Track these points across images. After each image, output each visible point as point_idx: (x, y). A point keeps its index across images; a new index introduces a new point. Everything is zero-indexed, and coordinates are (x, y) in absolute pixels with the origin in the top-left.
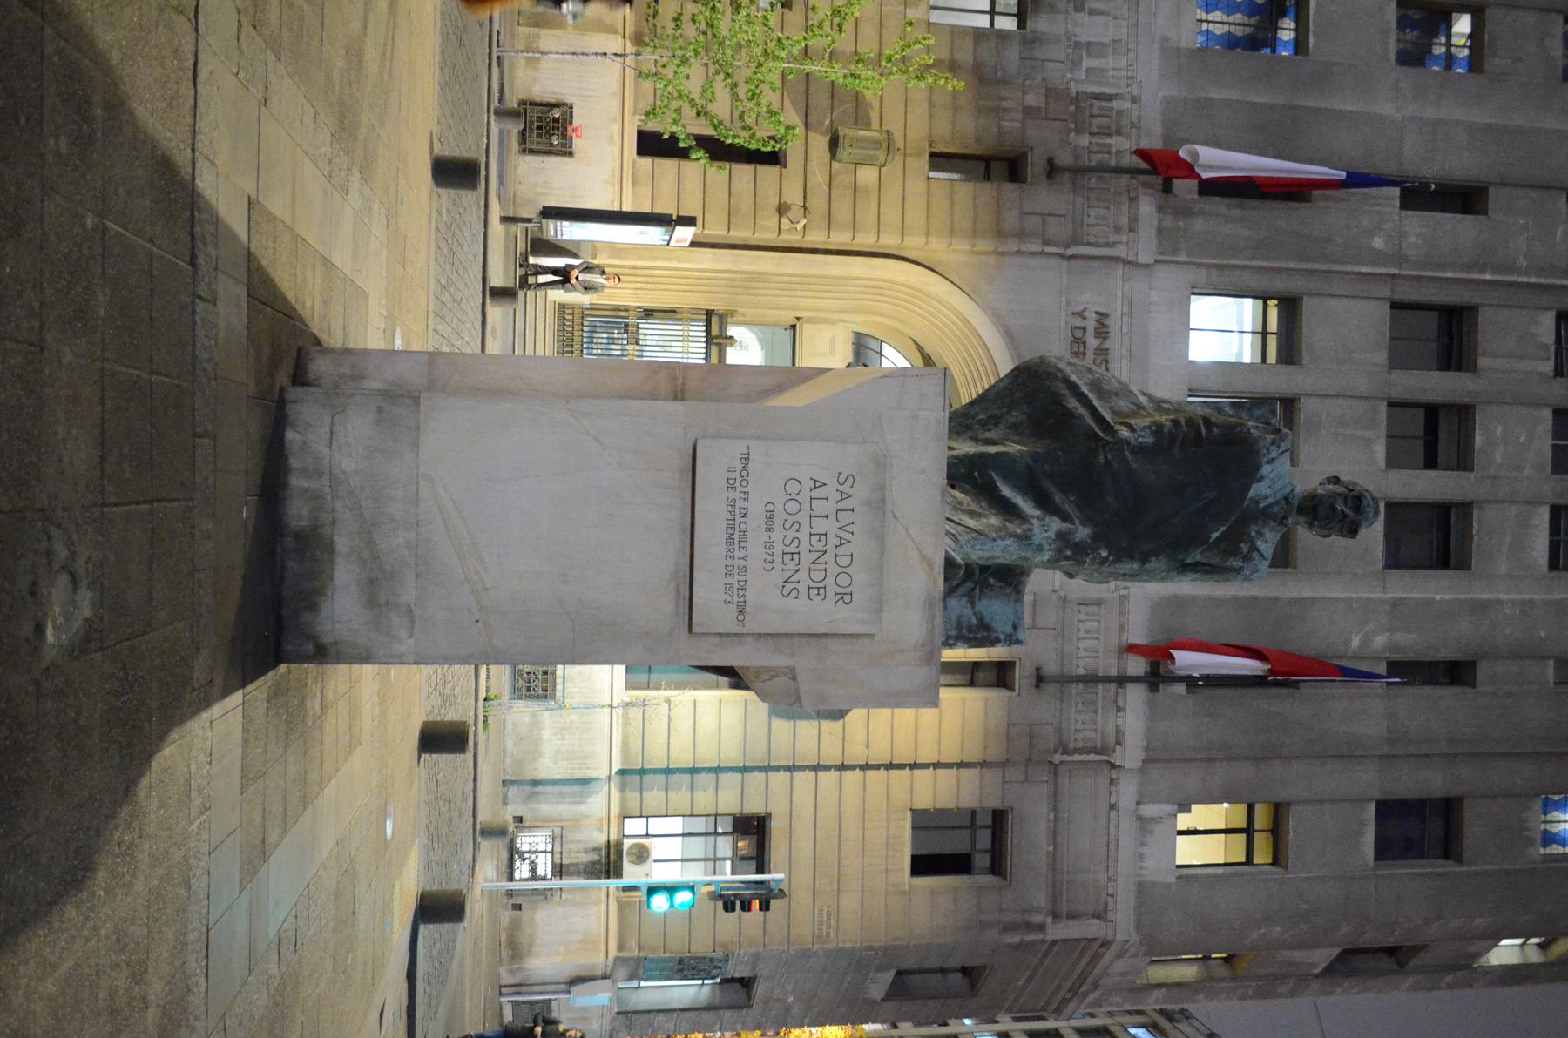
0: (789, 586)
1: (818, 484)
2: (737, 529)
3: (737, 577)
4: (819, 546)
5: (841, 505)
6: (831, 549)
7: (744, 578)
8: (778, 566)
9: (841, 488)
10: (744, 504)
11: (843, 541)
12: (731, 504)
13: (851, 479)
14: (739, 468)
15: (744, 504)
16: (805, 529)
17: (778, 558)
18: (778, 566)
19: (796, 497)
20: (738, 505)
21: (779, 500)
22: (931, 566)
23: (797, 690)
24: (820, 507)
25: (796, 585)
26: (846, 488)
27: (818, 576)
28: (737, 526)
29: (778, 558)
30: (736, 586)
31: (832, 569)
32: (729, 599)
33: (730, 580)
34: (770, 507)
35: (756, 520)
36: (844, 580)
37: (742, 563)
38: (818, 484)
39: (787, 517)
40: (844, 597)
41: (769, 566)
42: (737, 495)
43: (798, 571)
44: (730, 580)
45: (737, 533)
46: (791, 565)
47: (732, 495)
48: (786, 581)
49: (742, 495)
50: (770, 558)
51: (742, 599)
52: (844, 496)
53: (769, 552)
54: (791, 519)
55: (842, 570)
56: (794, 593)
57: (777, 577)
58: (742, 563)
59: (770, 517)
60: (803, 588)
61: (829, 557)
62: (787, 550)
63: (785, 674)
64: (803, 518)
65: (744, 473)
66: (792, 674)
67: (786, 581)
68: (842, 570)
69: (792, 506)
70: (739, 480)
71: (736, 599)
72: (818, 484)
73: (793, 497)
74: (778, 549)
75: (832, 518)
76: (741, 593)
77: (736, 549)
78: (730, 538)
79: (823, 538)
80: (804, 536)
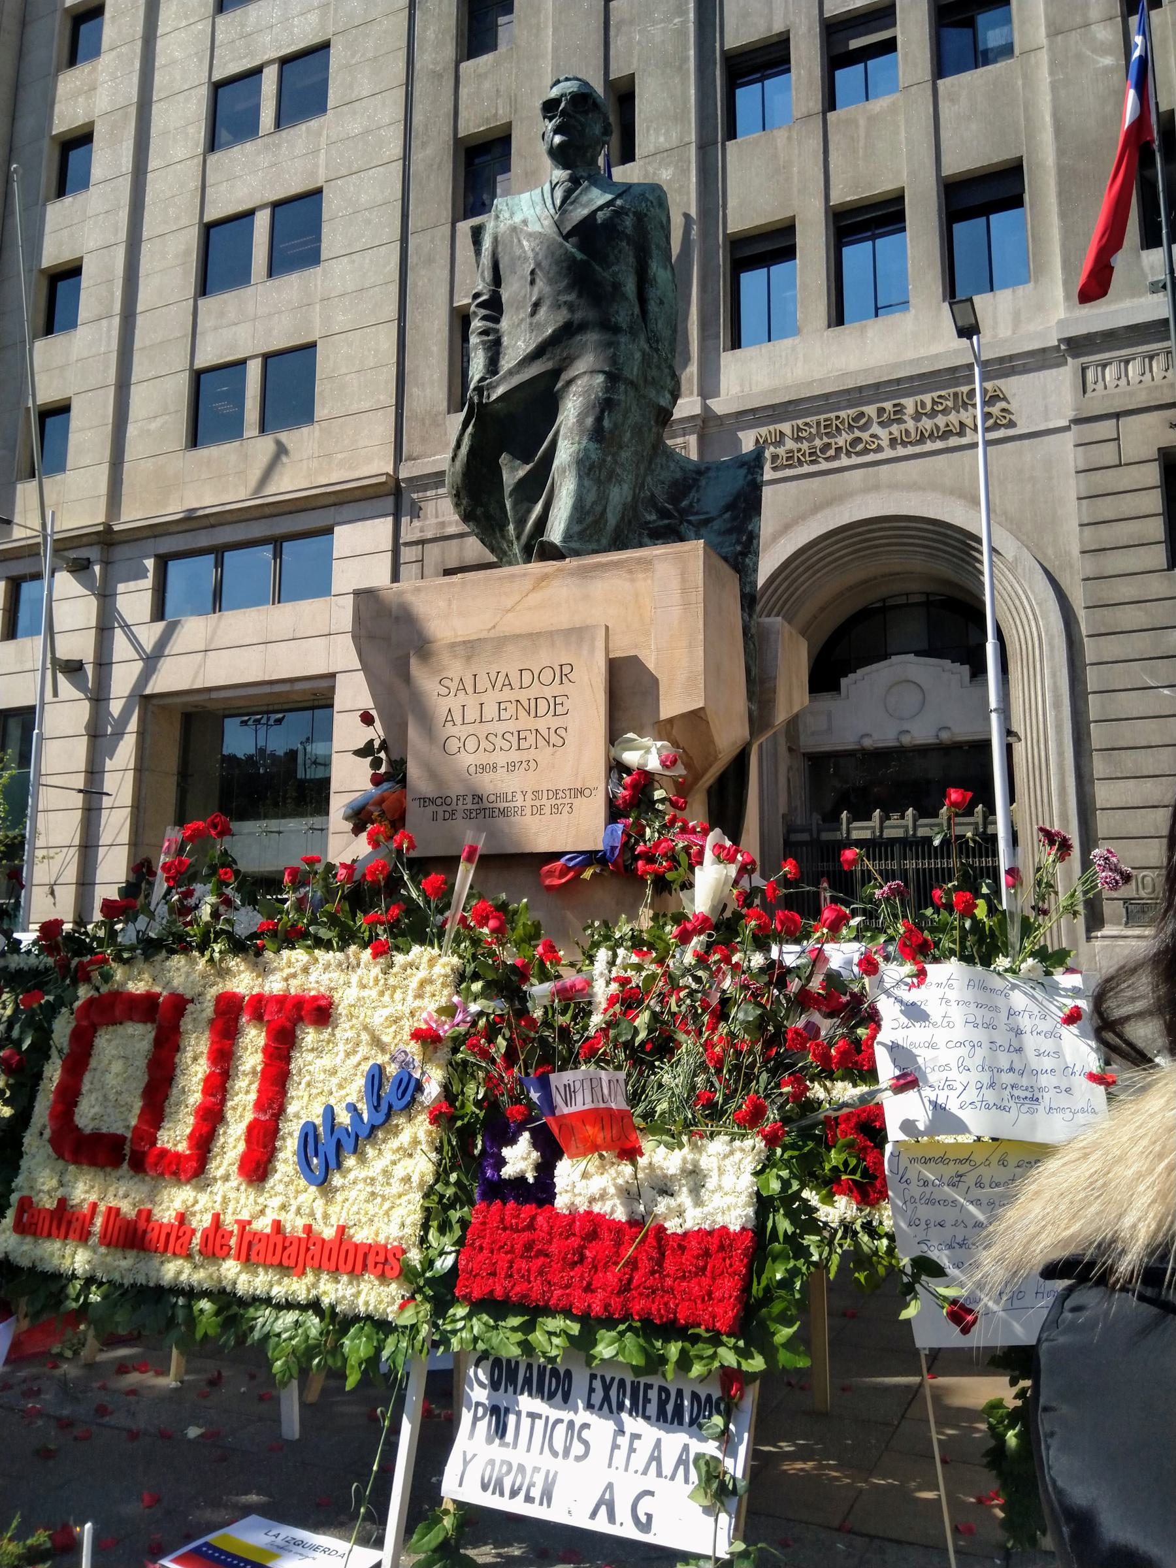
0: (554, 739)
3: (544, 801)
4: (512, 708)
5: (470, 690)
7: (545, 793)
11: (507, 682)
13: (445, 682)
14: (433, 808)
17: (524, 756)
20: (469, 806)
22: (545, 577)
24: (472, 714)
25: (552, 731)
26: (453, 686)
27: (542, 705)
29: (524, 756)
30: (553, 802)
31: (536, 690)
32: (567, 808)
33: (547, 810)
36: (547, 676)
37: (529, 796)
40: (563, 674)
41: (533, 764)
44: (547, 810)
46: (531, 739)
49: (460, 803)
50: (524, 764)
51: (568, 793)
52: (461, 687)
53: (517, 765)
54: (484, 744)
55: (536, 676)
56: (561, 732)
57: (544, 755)
58: (529, 796)
60: (555, 723)
61: (523, 696)
62: (515, 746)
65: (439, 802)
68: (536, 676)
70: (445, 808)
72: (449, 718)
73: (461, 745)
74: (514, 756)
75: (484, 698)
79: (502, 706)
80: (500, 728)
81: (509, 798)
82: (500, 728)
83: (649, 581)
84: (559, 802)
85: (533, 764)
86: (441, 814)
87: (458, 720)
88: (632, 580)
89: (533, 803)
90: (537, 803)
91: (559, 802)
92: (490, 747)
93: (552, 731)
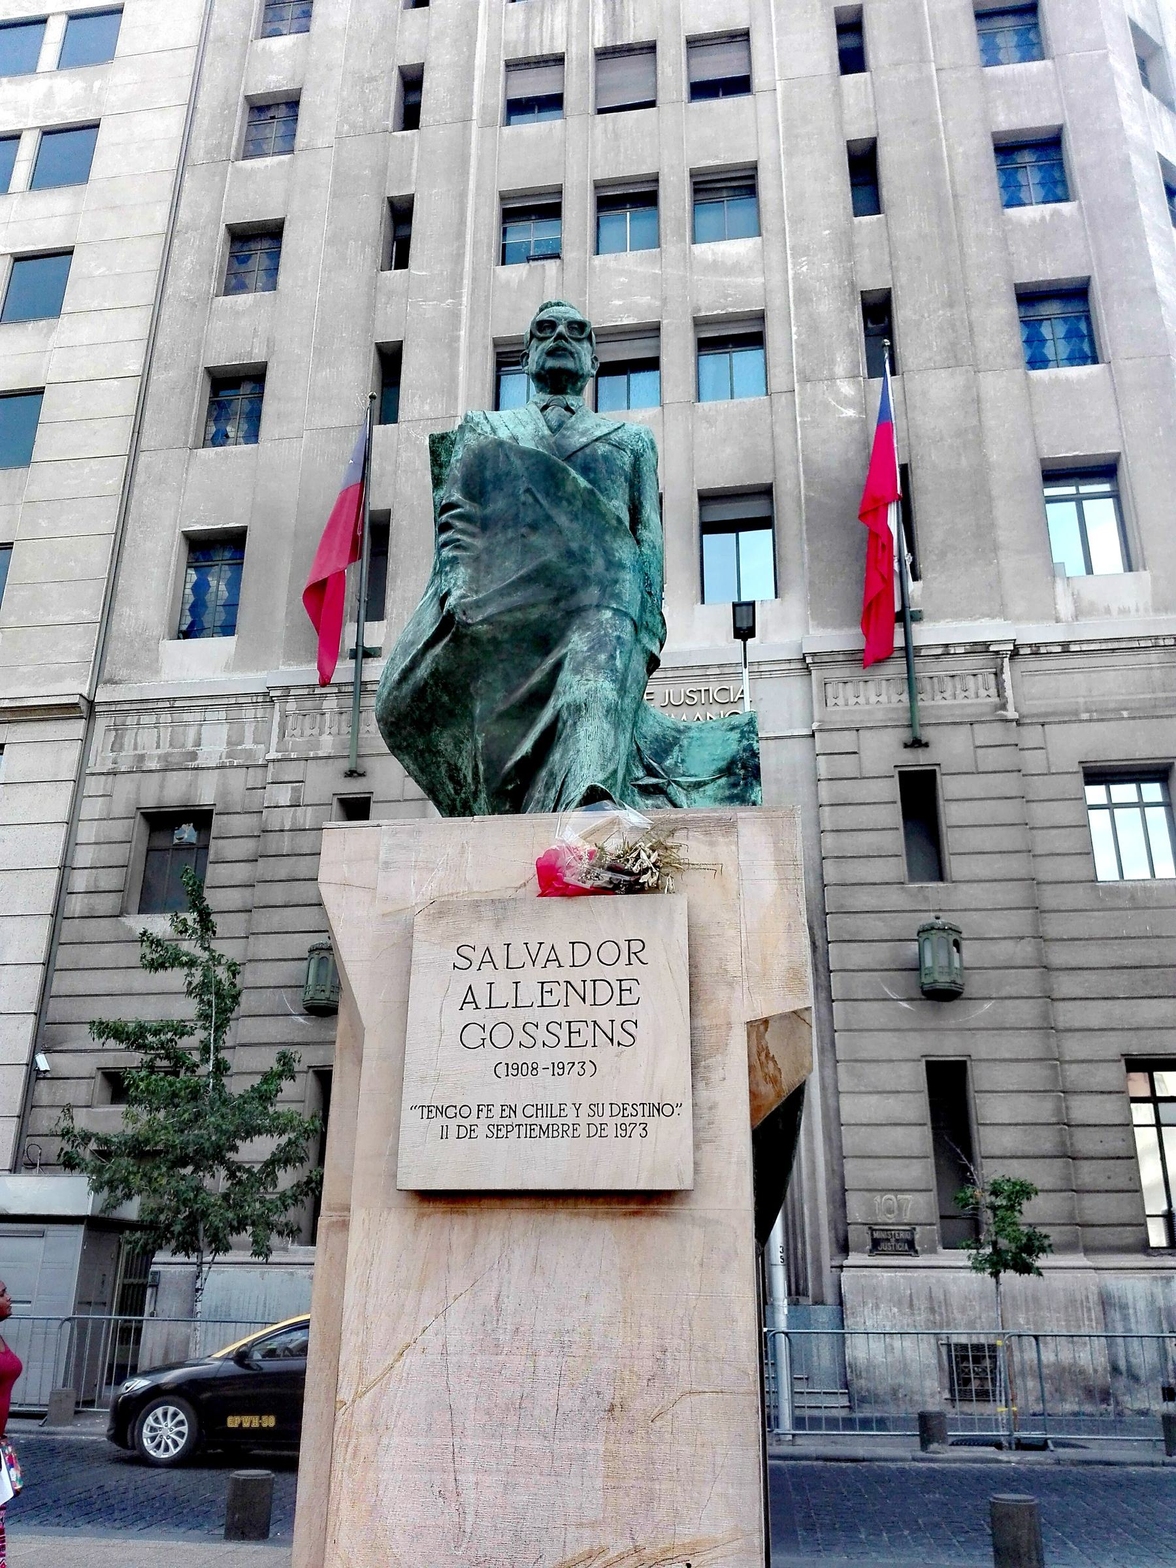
0: (619, 1035)
1: (469, 998)
2: (533, 1120)
4: (559, 992)
5: (501, 962)
6: (563, 975)
7: (607, 1108)
8: (588, 1053)
9: (475, 966)
10: (496, 1110)
11: (553, 957)
12: (496, 1131)
14: (441, 1120)
15: (496, 1110)
16: (537, 1014)
17: (576, 1055)
18: (588, 1053)
19: (488, 1030)
20: (496, 1120)
21: (492, 1056)
23: (783, 1017)
25: (617, 1025)
26: (476, 957)
27: (603, 992)
28: (529, 1121)
29: (576, 1055)
31: (594, 970)
32: (639, 1129)
33: (610, 1130)
34: (501, 1070)
35: (521, 1092)
36: (609, 953)
37: (584, 1110)
38: (470, 999)
39: (516, 1042)
40: (634, 952)
41: (589, 1068)
42: (483, 1122)
43: (595, 1022)
45: (539, 1121)
46: (587, 1033)
47: (481, 1131)
48: (612, 1040)
49: (483, 1115)
50: (577, 1067)
51: (640, 1109)
54: (520, 1036)
57: (604, 1054)
58: (584, 1110)
59: (517, 1069)
60: (621, 1014)
61: (576, 976)
63: (760, 1037)
64: (517, 1018)
66: (758, 1027)
67: (612, 1040)
69: (501, 1035)
71: (639, 1119)
72: (470, 999)
74: (563, 1054)
75: (519, 975)
76: (630, 1110)
77: (563, 1120)
78: (544, 1131)
79: (547, 987)
80: (542, 1016)
81: (556, 1112)
82: (542, 1016)
83: (734, 848)
84: (627, 1121)
85: (589, 1068)
86: (453, 1131)
87: (483, 1002)
88: (712, 844)
89: (590, 1120)
90: (597, 1120)
91: (627, 1121)
92: (529, 1042)
93: (617, 1025)
